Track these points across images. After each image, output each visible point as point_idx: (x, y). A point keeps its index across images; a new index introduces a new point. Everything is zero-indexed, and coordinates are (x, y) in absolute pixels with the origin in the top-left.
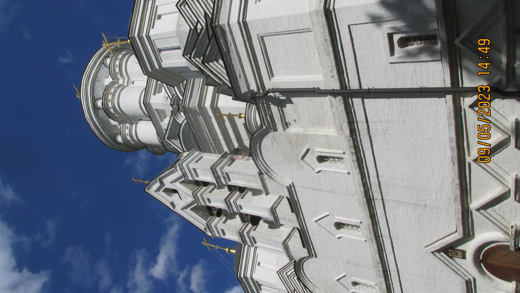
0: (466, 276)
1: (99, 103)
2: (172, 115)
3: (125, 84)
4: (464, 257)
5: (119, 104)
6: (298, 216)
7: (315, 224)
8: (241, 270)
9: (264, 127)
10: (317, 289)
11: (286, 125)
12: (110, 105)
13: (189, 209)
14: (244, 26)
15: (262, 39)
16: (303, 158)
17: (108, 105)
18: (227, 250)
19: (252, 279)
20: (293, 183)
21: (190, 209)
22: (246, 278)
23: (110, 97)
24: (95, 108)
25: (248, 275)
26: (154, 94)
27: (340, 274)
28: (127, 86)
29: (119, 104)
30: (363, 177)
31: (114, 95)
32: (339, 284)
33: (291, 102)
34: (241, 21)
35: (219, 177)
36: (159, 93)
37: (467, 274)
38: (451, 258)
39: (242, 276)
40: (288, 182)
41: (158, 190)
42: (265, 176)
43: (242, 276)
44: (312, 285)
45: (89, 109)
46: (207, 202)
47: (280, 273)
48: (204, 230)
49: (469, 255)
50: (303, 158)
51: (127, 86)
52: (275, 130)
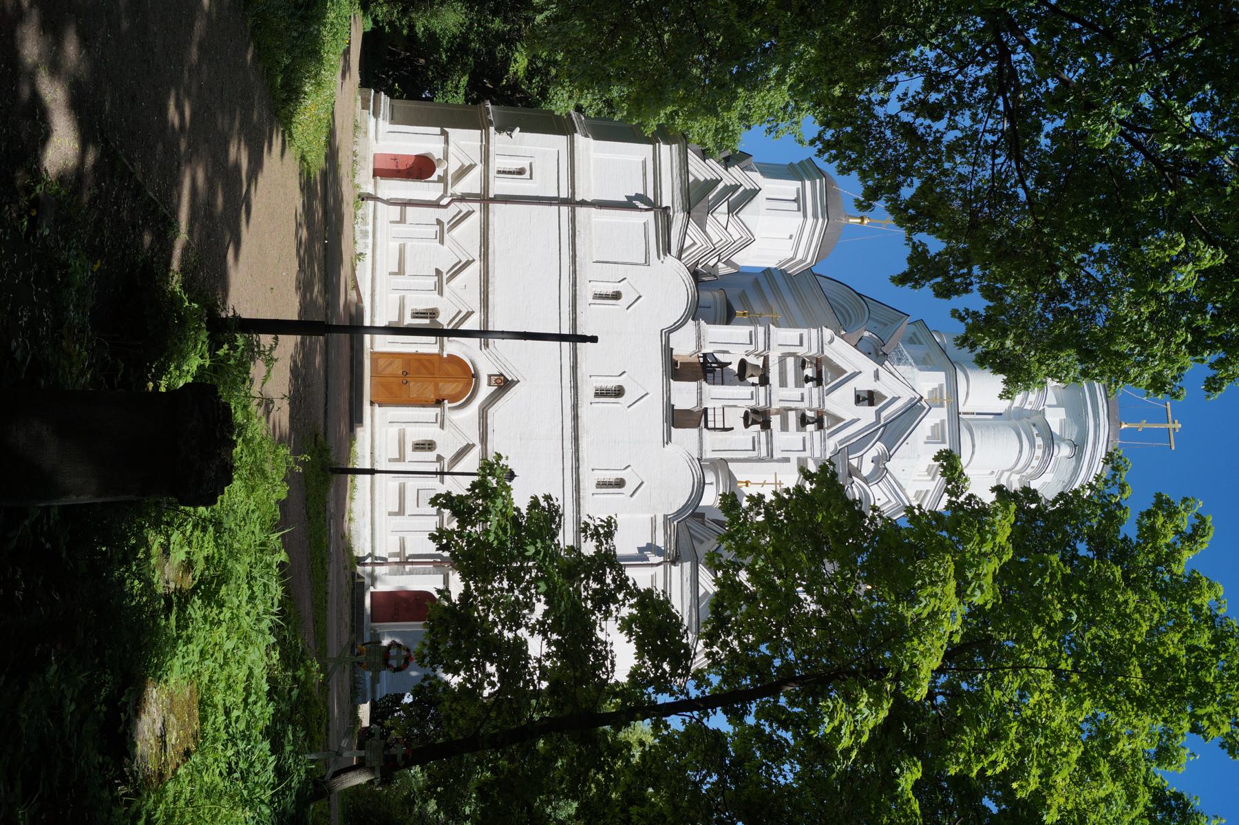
1: (1064, 451)
2: (890, 457)
3: (1006, 475)
4: (490, 376)
5: (1021, 452)
6: (669, 398)
8: (821, 229)
9: (675, 523)
11: (653, 521)
12: (1039, 452)
13: (850, 372)
16: (642, 483)
17: (1044, 452)
18: (866, 222)
19: (805, 216)
21: (846, 372)
22: (815, 216)
23: (1035, 463)
24: (1078, 447)
25: (810, 220)
28: (1003, 472)
29: (1021, 452)
30: (578, 468)
31: (1027, 466)
32: (639, 290)
33: (639, 548)
35: (767, 444)
38: (502, 375)
39: (820, 220)
40: (669, 447)
41: (895, 399)
42: (696, 456)
43: (820, 220)
45: (1094, 444)
48: (836, 337)
49: (484, 380)
50: (642, 483)
51: (1003, 472)
52: (665, 516)
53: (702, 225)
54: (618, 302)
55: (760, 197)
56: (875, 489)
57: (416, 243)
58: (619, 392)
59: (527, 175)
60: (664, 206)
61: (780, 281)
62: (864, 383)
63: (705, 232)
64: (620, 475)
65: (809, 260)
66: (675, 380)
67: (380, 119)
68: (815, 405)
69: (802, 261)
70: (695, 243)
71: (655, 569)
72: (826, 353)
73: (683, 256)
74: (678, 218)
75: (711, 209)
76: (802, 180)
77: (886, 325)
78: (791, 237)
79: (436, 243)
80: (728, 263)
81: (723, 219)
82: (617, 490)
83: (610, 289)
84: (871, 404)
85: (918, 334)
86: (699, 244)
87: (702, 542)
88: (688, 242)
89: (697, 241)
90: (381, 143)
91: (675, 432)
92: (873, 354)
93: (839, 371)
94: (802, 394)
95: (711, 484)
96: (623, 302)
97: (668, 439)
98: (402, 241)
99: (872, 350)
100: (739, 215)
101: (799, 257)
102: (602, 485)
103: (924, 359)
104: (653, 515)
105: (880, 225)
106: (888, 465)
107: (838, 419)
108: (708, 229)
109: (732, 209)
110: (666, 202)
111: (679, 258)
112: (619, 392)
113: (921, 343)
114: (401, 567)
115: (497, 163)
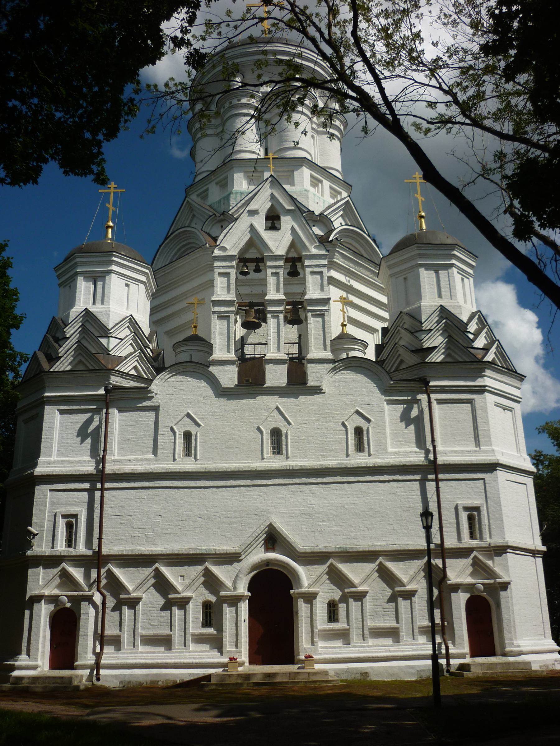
0: (245, 553)
2: (310, 211)
7: (274, 407)
9: (392, 382)
10: (161, 383)
14: (482, 390)
15: (470, 401)
16: (358, 412)
18: (111, 224)
19: (110, 272)
20: (324, 393)
26: (312, 176)
27: (199, 419)
32: (183, 415)
34: (487, 388)
36: (311, 181)
37: (246, 554)
40: (325, 388)
42: (331, 366)
44: (166, 377)
46: (274, 270)
47: (130, 319)
53: (120, 360)
54: (193, 433)
55: (92, 308)
56: (336, 224)
57: (140, 625)
58: (276, 434)
59: (74, 520)
60: (104, 392)
61: (158, 302)
62: (260, 223)
63: (126, 357)
64: (351, 432)
65: (148, 271)
66: (264, 383)
67: (17, 663)
68: (282, 263)
69: (147, 278)
70: (135, 368)
71: (432, 400)
72: (235, 253)
73: (146, 377)
74: (115, 380)
75: (106, 351)
76: (77, 274)
77: (194, 216)
78: (127, 285)
79: (140, 607)
80: (150, 339)
81: (113, 342)
82: (365, 434)
83: (180, 441)
84: (279, 218)
85: (198, 192)
86: (136, 363)
87: (402, 361)
88: (133, 372)
89: (133, 365)
90: (39, 663)
91: (312, 382)
92: (224, 224)
93: (250, 244)
94: (272, 273)
95: (347, 355)
96: (193, 430)
97: (317, 390)
98: (138, 639)
99: (219, 225)
100: (110, 328)
101: (143, 279)
102: (360, 447)
103: (221, 186)
104: (385, 403)
105: (114, 213)
106: (317, 213)
107: (292, 245)
108: (123, 355)
109: (106, 333)
110: (102, 392)
111: (149, 381)
112: (276, 434)
113: (207, 190)
114: (447, 631)
115: (61, 547)
